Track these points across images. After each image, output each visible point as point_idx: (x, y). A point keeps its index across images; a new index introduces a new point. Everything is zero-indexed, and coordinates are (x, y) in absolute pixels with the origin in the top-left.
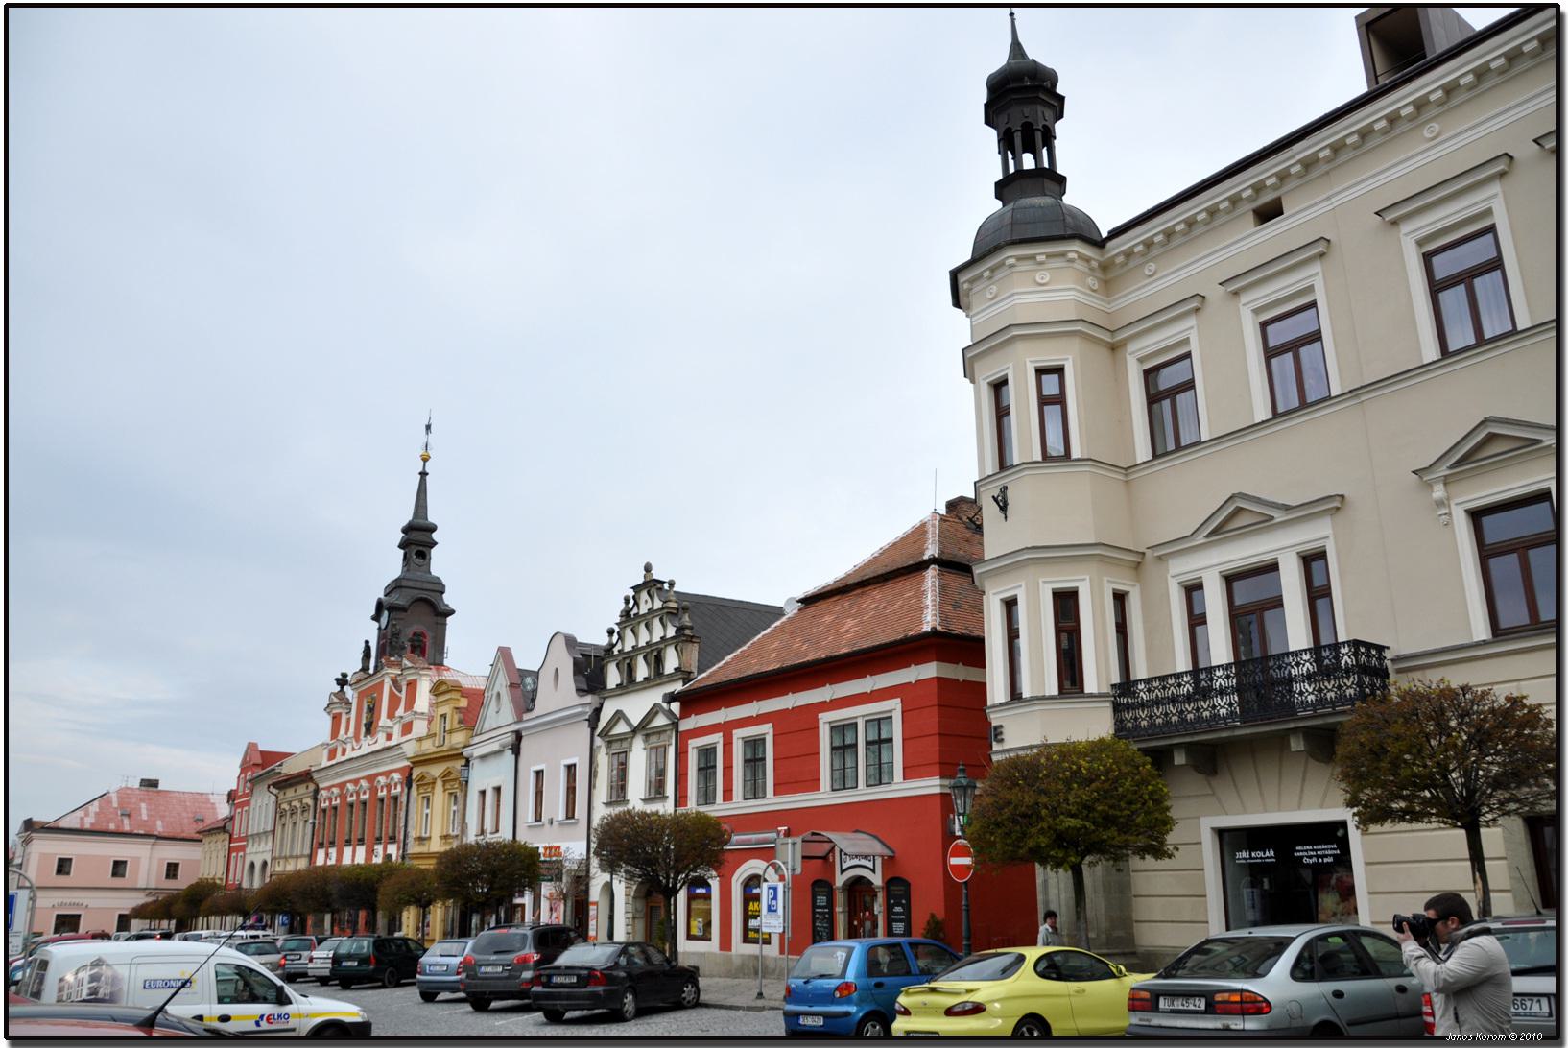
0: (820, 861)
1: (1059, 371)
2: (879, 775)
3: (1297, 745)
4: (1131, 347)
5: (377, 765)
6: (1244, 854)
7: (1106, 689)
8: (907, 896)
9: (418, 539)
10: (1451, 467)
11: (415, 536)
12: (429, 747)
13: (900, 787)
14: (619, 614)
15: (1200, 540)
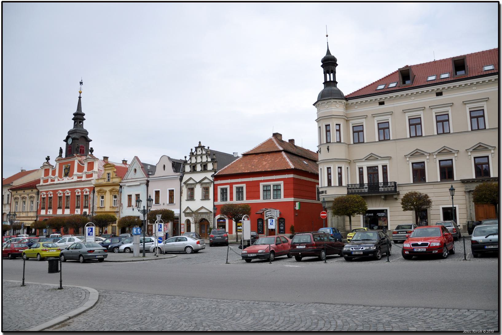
0: (260, 215)
1: (339, 125)
2: (277, 196)
3: (383, 197)
4: (351, 121)
5: (75, 186)
6: (367, 214)
7: (346, 185)
8: (284, 222)
9: (79, 117)
10: (410, 156)
11: (79, 117)
12: (102, 182)
13: (283, 199)
14: (190, 153)
15: (364, 160)
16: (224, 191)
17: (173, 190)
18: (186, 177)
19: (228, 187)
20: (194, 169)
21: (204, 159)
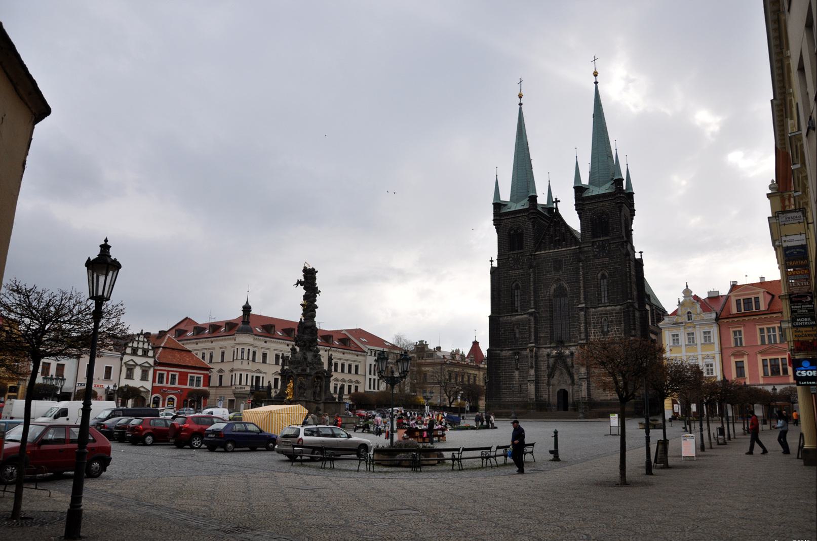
16: (161, 376)
17: (111, 368)
18: (126, 358)
19: (165, 373)
20: (134, 352)
21: (146, 346)
